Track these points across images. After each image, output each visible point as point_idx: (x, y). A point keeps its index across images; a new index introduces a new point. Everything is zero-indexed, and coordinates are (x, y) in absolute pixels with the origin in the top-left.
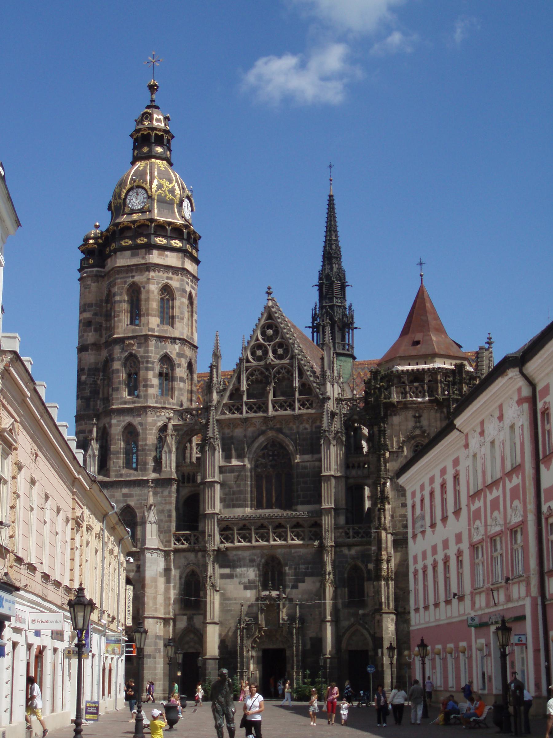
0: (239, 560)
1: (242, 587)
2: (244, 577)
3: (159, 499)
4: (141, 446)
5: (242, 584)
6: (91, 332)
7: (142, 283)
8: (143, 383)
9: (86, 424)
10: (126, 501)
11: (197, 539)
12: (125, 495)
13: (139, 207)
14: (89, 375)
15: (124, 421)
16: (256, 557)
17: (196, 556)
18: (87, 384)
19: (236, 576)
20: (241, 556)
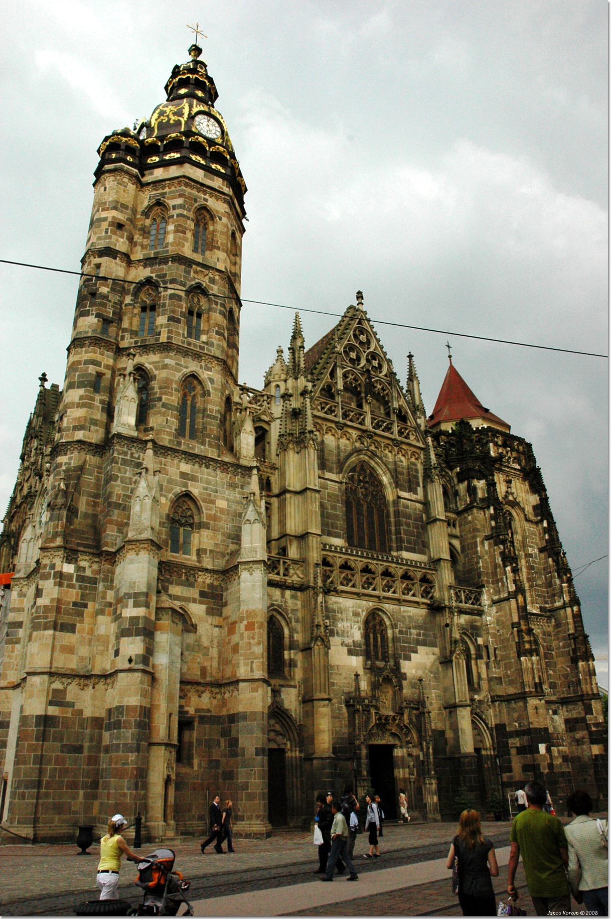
0: (341, 611)
1: (345, 649)
2: (348, 636)
3: (237, 495)
4: (212, 411)
5: (346, 646)
6: (123, 238)
7: (217, 212)
8: (217, 329)
9: (103, 355)
10: (186, 485)
11: (286, 569)
12: (184, 475)
13: (210, 136)
14: (113, 290)
15: (186, 367)
16: (360, 610)
17: (283, 596)
18: (110, 301)
19: (338, 633)
20: (342, 605)
